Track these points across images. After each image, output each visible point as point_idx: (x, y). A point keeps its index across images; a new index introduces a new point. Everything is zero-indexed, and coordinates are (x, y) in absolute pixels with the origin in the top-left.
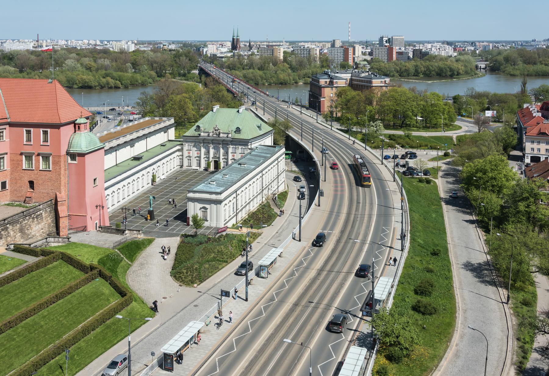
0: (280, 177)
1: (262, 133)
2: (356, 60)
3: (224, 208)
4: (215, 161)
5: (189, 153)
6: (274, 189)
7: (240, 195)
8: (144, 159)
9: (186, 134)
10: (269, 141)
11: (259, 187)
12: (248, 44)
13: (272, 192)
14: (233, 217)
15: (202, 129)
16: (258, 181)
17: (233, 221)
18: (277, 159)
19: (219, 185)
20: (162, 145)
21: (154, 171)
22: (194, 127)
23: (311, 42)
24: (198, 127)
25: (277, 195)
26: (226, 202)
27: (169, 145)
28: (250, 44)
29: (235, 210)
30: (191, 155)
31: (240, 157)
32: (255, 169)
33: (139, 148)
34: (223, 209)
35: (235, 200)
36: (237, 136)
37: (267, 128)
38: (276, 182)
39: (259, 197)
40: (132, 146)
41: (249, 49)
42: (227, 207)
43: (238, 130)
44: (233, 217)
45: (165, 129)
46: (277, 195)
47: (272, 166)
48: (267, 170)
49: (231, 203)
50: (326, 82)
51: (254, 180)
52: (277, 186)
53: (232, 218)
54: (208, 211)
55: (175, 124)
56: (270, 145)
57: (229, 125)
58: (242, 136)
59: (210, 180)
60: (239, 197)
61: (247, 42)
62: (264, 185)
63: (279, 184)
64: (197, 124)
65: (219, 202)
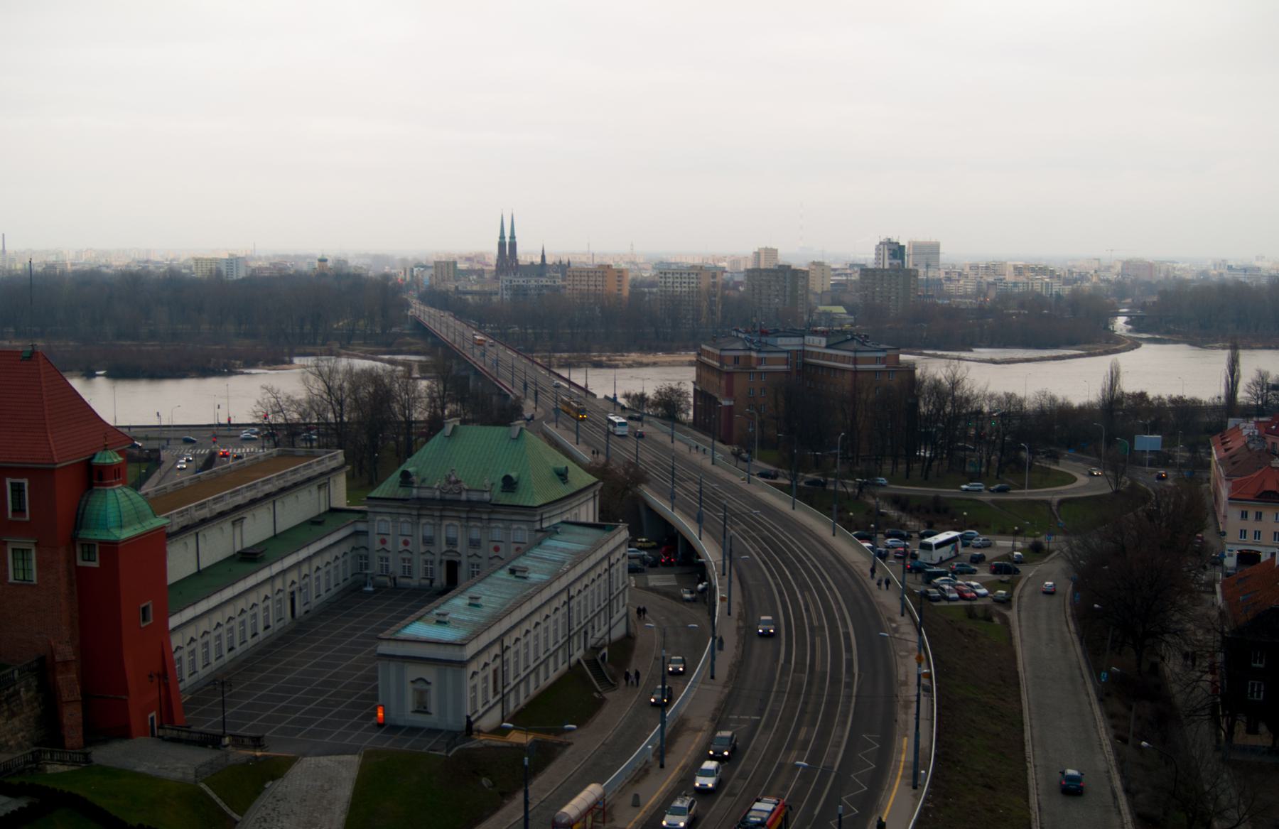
3: (472, 684)
5: (383, 542)
6: (598, 635)
7: (513, 649)
10: (587, 511)
19: (459, 624)
20: (315, 522)
21: (295, 587)
22: (396, 475)
24: (406, 475)
25: (605, 650)
30: (389, 546)
32: (549, 583)
33: (256, 528)
34: (469, 684)
35: (498, 661)
36: (505, 499)
37: (581, 478)
40: (238, 522)
42: (478, 680)
43: (509, 484)
45: (321, 480)
46: (605, 650)
47: (593, 575)
48: (579, 586)
49: (490, 670)
53: (491, 708)
55: (348, 468)
56: (591, 520)
60: (510, 655)
63: (613, 621)
64: (402, 468)
65: (463, 664)
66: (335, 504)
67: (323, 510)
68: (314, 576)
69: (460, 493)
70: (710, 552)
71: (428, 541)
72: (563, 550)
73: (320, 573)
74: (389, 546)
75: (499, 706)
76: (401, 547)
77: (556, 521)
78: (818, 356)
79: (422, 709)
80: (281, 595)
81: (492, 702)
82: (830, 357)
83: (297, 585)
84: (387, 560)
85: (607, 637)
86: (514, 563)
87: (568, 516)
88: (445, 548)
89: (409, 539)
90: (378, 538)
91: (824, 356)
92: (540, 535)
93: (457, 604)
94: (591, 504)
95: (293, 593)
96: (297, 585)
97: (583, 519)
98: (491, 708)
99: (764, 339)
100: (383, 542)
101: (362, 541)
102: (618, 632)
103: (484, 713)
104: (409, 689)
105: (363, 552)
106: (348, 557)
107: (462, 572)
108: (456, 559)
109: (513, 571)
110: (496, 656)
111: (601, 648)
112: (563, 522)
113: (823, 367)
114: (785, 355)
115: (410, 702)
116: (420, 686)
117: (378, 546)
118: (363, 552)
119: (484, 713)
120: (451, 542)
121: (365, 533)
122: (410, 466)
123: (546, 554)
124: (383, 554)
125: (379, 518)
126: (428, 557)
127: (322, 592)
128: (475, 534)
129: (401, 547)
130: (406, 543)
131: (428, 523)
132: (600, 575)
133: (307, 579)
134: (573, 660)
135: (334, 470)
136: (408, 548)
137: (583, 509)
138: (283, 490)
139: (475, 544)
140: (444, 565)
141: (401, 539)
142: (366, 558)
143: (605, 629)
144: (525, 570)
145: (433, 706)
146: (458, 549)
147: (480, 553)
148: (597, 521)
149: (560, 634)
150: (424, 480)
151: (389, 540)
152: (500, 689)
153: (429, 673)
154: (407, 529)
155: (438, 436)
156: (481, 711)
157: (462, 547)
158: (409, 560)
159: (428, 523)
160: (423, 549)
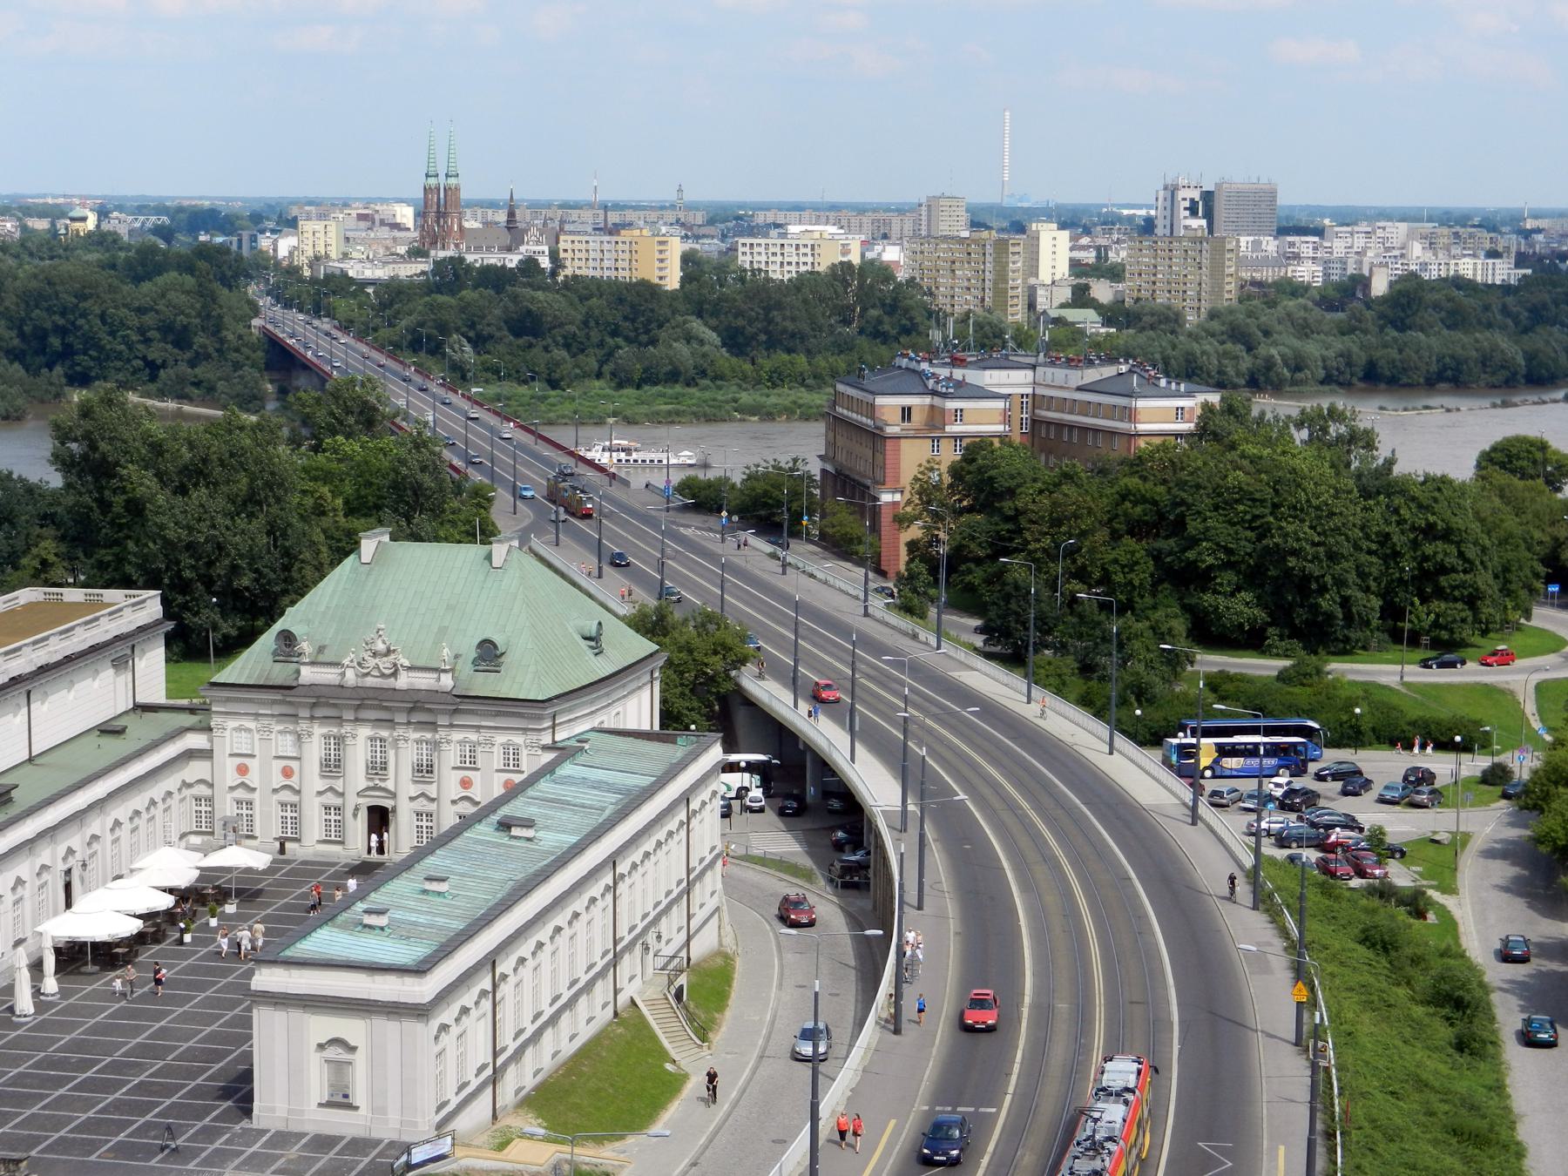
0: (698, 893)
1: (603, 667)
2: (1042, 303)
4: (371, 809)
5: (242, 770)
6: (669, 950)
7: (512, 980)
8: (21, 798)
9: (220, 678)
10: (639, 708)
11: (602, 942)
12: (502, 217)
13: (660, 962)
15: (306, 647)
16: (596, 910)
18: (685, 798)
20: (109, 730)
21: (71, 862)
22: (267, 641)
23: (816, 208)
24: (287, 638)
26: (447, 1015)
27: (142, 731)
28: (511, 214)
30: (253, 779)
31: (498, 791)
35: (486, 1004)
36: (485, 685)
38: (678, 914)
39: (602, 991)
41: (506, 239)
43: (489, 655)
48: (636, 856)
50: (906, 413)
51: (579, 904)
52: (683, 936)
54: (360, 1058)
55: (170, 626)
56: (646, 727)
57: (443, 631)
58: (510, 683)
59: (360, 906)
60: (505, 990)
61: (493, 205)
62: (623, 931)
63: (694, 924)
64: (278, 626)
66: (141, 699)
70: (877, 787)
72: (597, 785)
75: (489, 1090)
76: (278, 781)
77: (580, 728)
78: (1062, 404)
79: (341, 1101)
82: (1085, 408)
86: (505, 811)
87: (608, 719)
88: (362, 783)
91: (1073, 406)
92: (549, 757)
93: (397, 892)
94: (646, 693)
95: (68, 872)
96: (78, 856)
97: (632, 725)
99: (958, 374)
100: (242, 770)
105: (203, 790)
107: (403, 836)
108: (388, 803)
109: (505, 826)
110: (483, 993)
112: (593, 730)
113: (1071, 427)
114: (1000, 404)
115: (317, 1086)
116: (334, 1053)
117: (232, 778)
118: (203, 790)
121: (207, 754)
122: (293, 618)
123: (567, 792)
124: (241, 794)
130: (287, 773)
132: (670, 834)
134: (623, 999)
135: (142, 629)
136: (294, 782)
138: (44, 670)
142: (210, 800)
144: (528, 823)
145: (360, 1097)
147: (432, 791)
148: (657, 727)
150: (321, 649)
151: (252, 764)
153: (351, 1028)
154: (286, 745)
155: (349, 562)
160: (321, 785)
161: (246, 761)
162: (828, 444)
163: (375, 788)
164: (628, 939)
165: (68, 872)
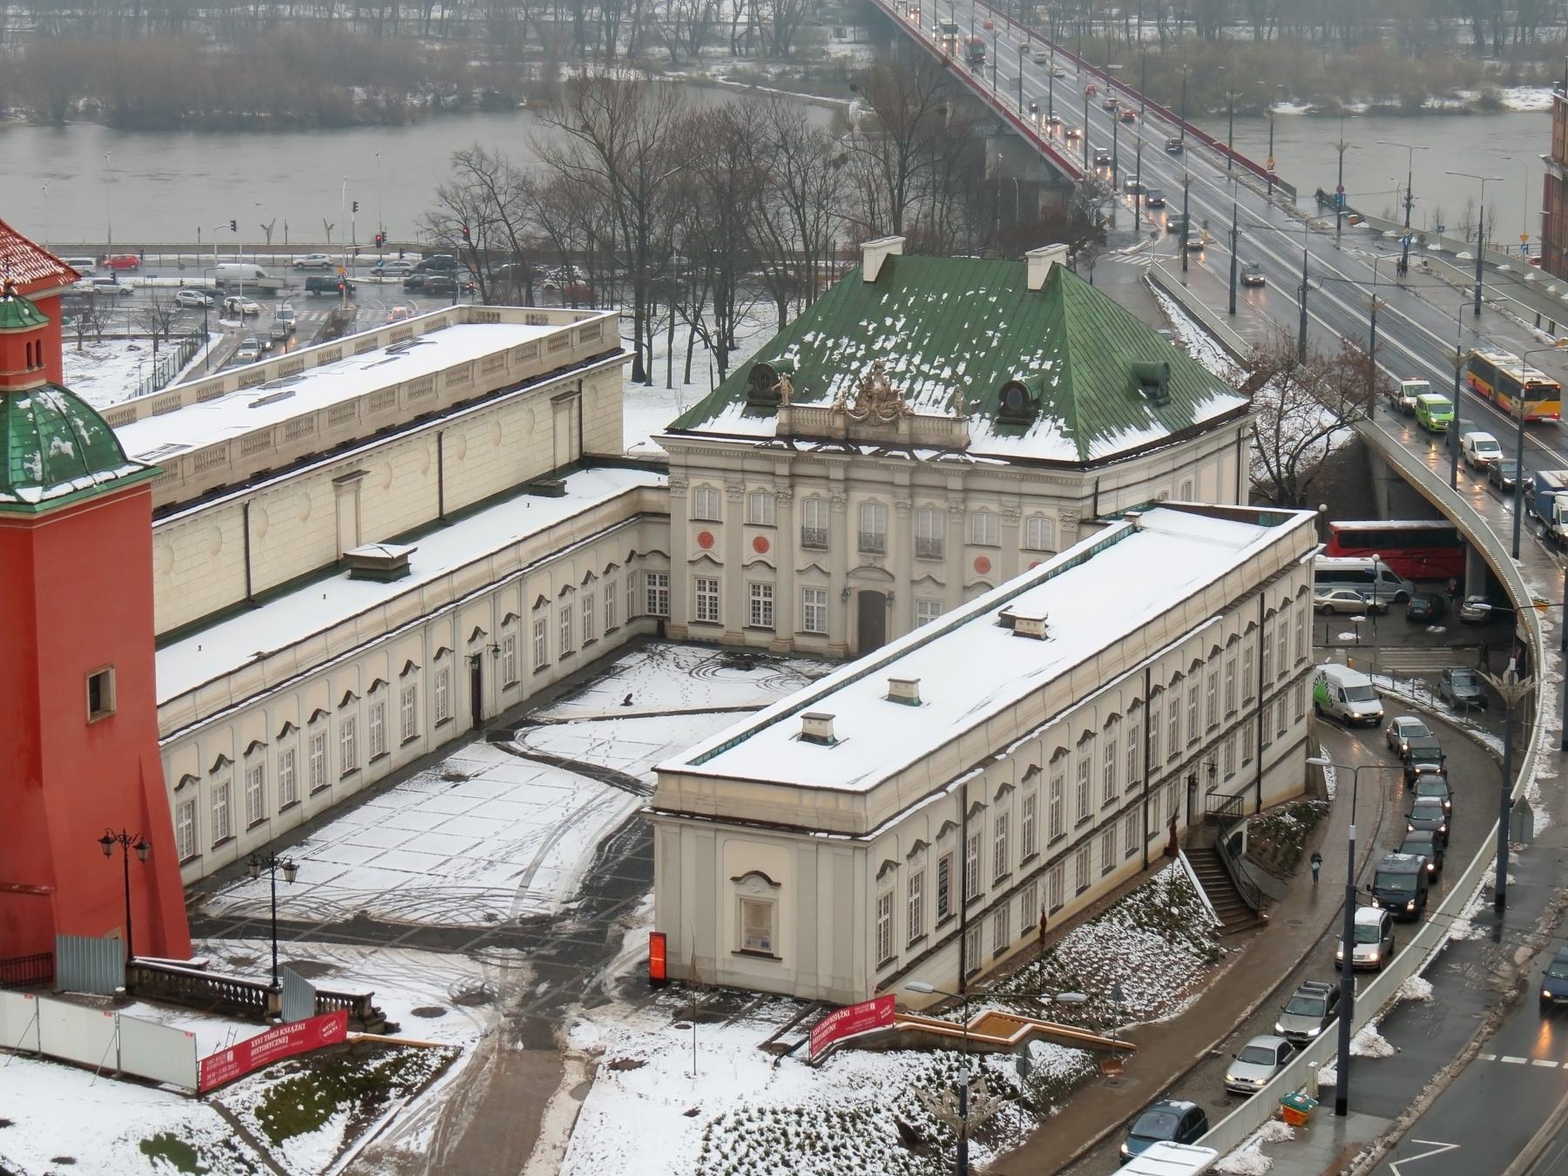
3: (883, 890)
5: (706, 540)
14: (940, 946)
17: (941, 973)
21: (481, 645)
29: (955, 906)
44: (940, 946)
46: (1243, 828)
53: (929, 954)
67: (563, 459)
68: (530, 618)
69: (895, 424)
71: (814, 542)
73: (545, 611)
74: (719, 551)
75: (954, 948)
76: (750, 555)
80: (446, 660)
81: (934, 938)
83: (488, 639)
84: (714, 585)
85: (1249, 799)
88: (855, 560)
89: (768, 535)
90: (692, 533)
95: (476, 659)
96: (488, 639)
98: (929, 954)
100: (706, 540)
101: (654, 537)
102: (1283, 783)
103: (910, 967)
104: (729, 897)
105: (656, 564)
106: (620, 576)
108: (883, 588)
111: (1234, 820)
117: (693, 550)
118: (656, 564)
119: (910, 967)
120: (872, 546)
125: (695, 482)
126: (815, 580)
127: (553, 656)
128: (930, 528)
129: (750, 555)
130: (761, 545)
131: (816, 497)
133: (513, 627)
136: (767, 557)
137: (1208, 471)
139: (929, 551)
140: (854, 601)
141: (750, 535)
142: (665, 579)
143: (1245, 775)
145: (784, 944)
146: (888, 564)
147: (939, 573)
149: (1122, 783)
152: (955, 906)
154: (763, 509)
156: (904, 959)
157: (896, 558)
158: (768, 590)
159: (816, 497)
160: (802, 560)
161: (711, 529)
162: (1555, 140)
163: (870, 568)
164: (1166, 771)
165: (476, 659)
